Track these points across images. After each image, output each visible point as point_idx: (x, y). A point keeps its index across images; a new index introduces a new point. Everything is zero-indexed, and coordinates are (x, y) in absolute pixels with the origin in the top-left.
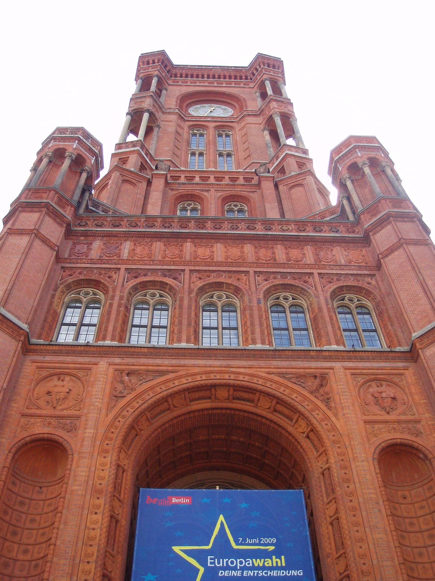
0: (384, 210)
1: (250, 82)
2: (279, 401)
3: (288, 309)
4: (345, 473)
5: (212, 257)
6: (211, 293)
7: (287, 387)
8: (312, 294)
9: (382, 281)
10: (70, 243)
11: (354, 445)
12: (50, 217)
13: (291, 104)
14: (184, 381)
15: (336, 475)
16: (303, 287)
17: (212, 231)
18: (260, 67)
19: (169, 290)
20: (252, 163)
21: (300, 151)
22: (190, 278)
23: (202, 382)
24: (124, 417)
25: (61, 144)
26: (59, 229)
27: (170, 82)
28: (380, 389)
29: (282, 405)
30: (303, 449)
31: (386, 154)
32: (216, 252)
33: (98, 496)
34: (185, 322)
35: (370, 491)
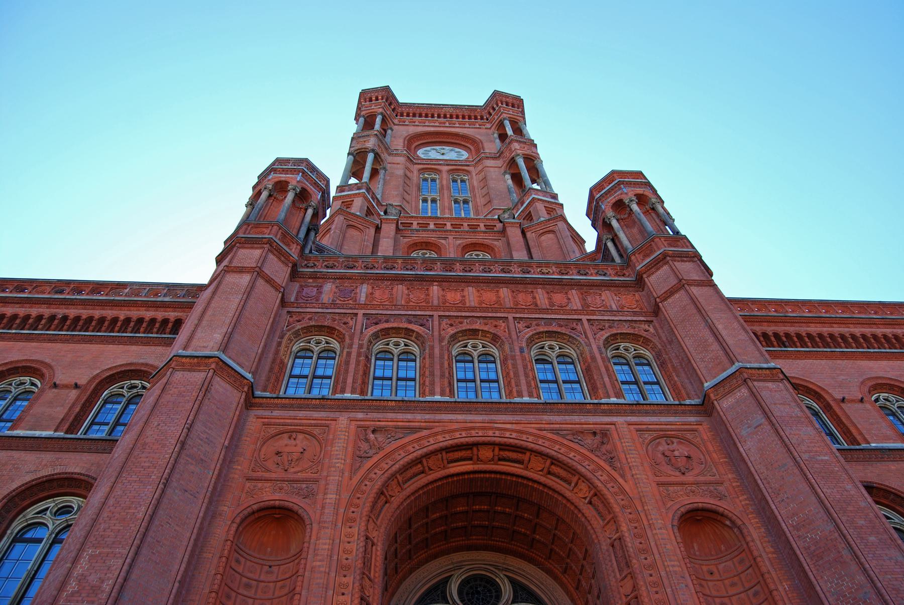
0: (659, 249)
1: (486, 122)
2: (554, 461)
3: (555, 359)
4: (641, 543)
5: (463, 302)
6: (465, 342)
7: (562, 444)
8: (583, 342)
9: (662, 328)
10: (296, 286)
11: (649, 510)
12: (274, 255)
13: (535, 146)
14: (440, 438)
15: (630, 545)
16: (571, 334)
17: (462, 274)
18: (497, 105)
19: (416, 338)
20: (494, 209)
21: (548, 195)
22: (440, 324)
23: (462, 440)
24: (371, 480)
25: (283, 177)
26: (285, 269)
27: (396, 121)
28: (671, 447)
29: (558, 466)
30: (586, 518)
31: (654, 191)
32: (467, 297)
33: (345, 573)
34: (437, 373)
35: (673, 563)
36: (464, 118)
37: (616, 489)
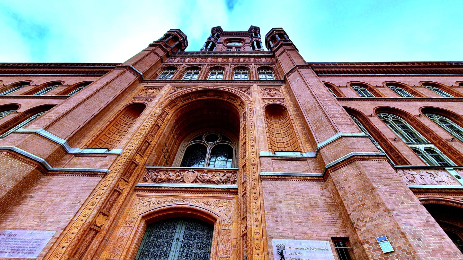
36: (242, 34)
37: (248, 99)
